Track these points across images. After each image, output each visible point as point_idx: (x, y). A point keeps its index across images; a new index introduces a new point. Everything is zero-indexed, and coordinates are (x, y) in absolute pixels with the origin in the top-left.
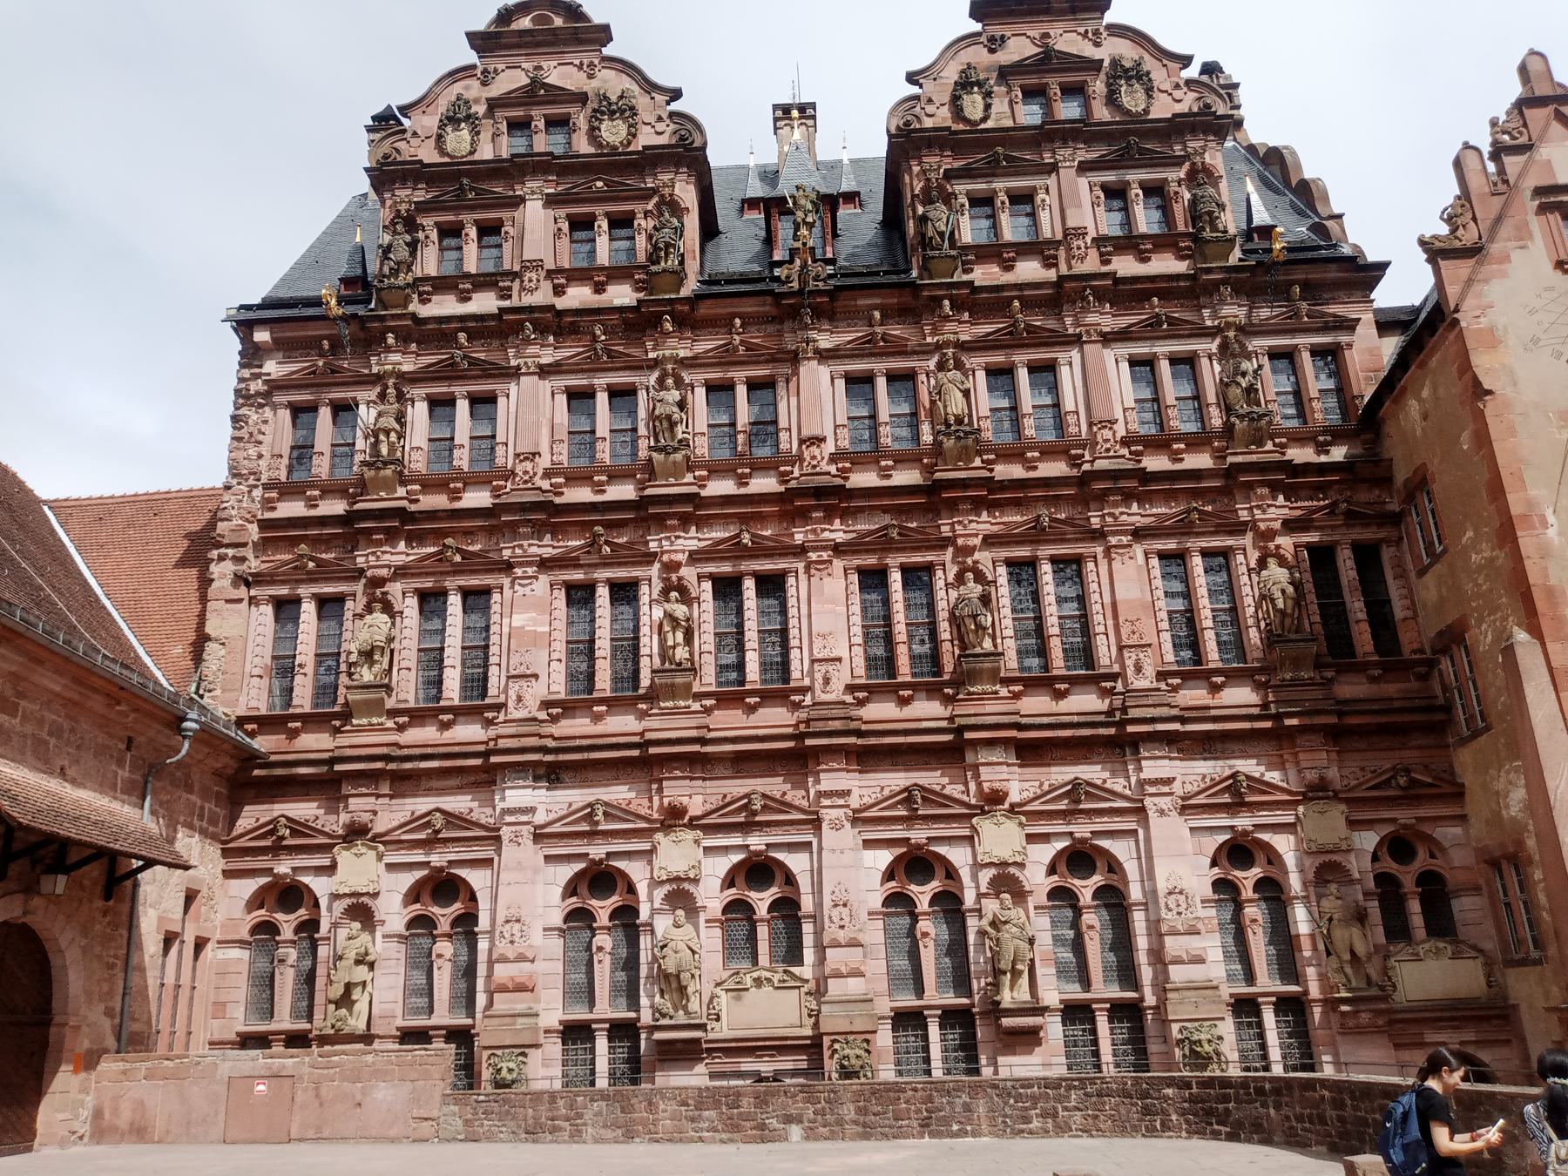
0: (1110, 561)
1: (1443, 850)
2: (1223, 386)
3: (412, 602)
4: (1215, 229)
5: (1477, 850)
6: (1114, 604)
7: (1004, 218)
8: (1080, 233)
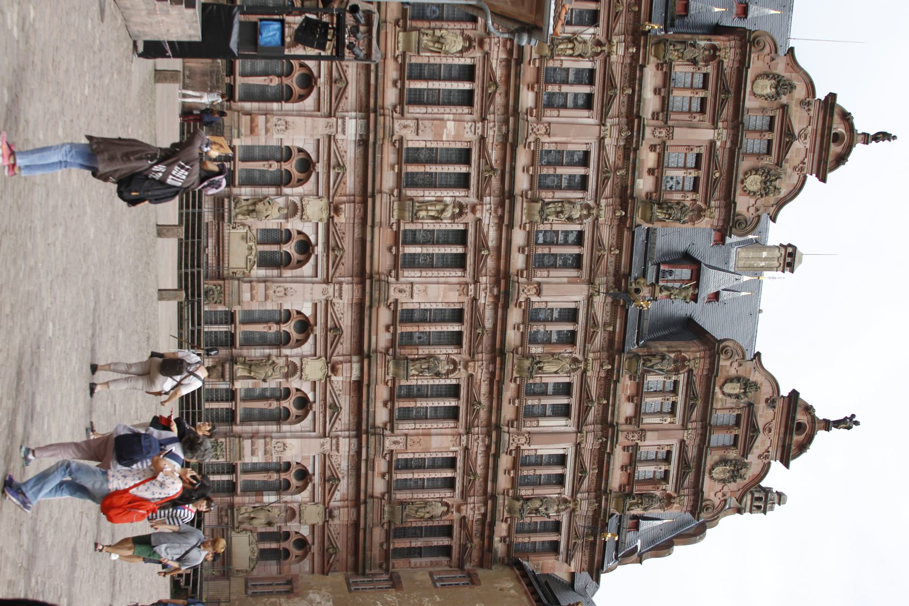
0: (453, 435)
1: (299, 561)
2: (542, 499)
3: (468, 62)
4: (632, 505)
5: (297, 576)
6: (430, 435)
8: (642, 437)
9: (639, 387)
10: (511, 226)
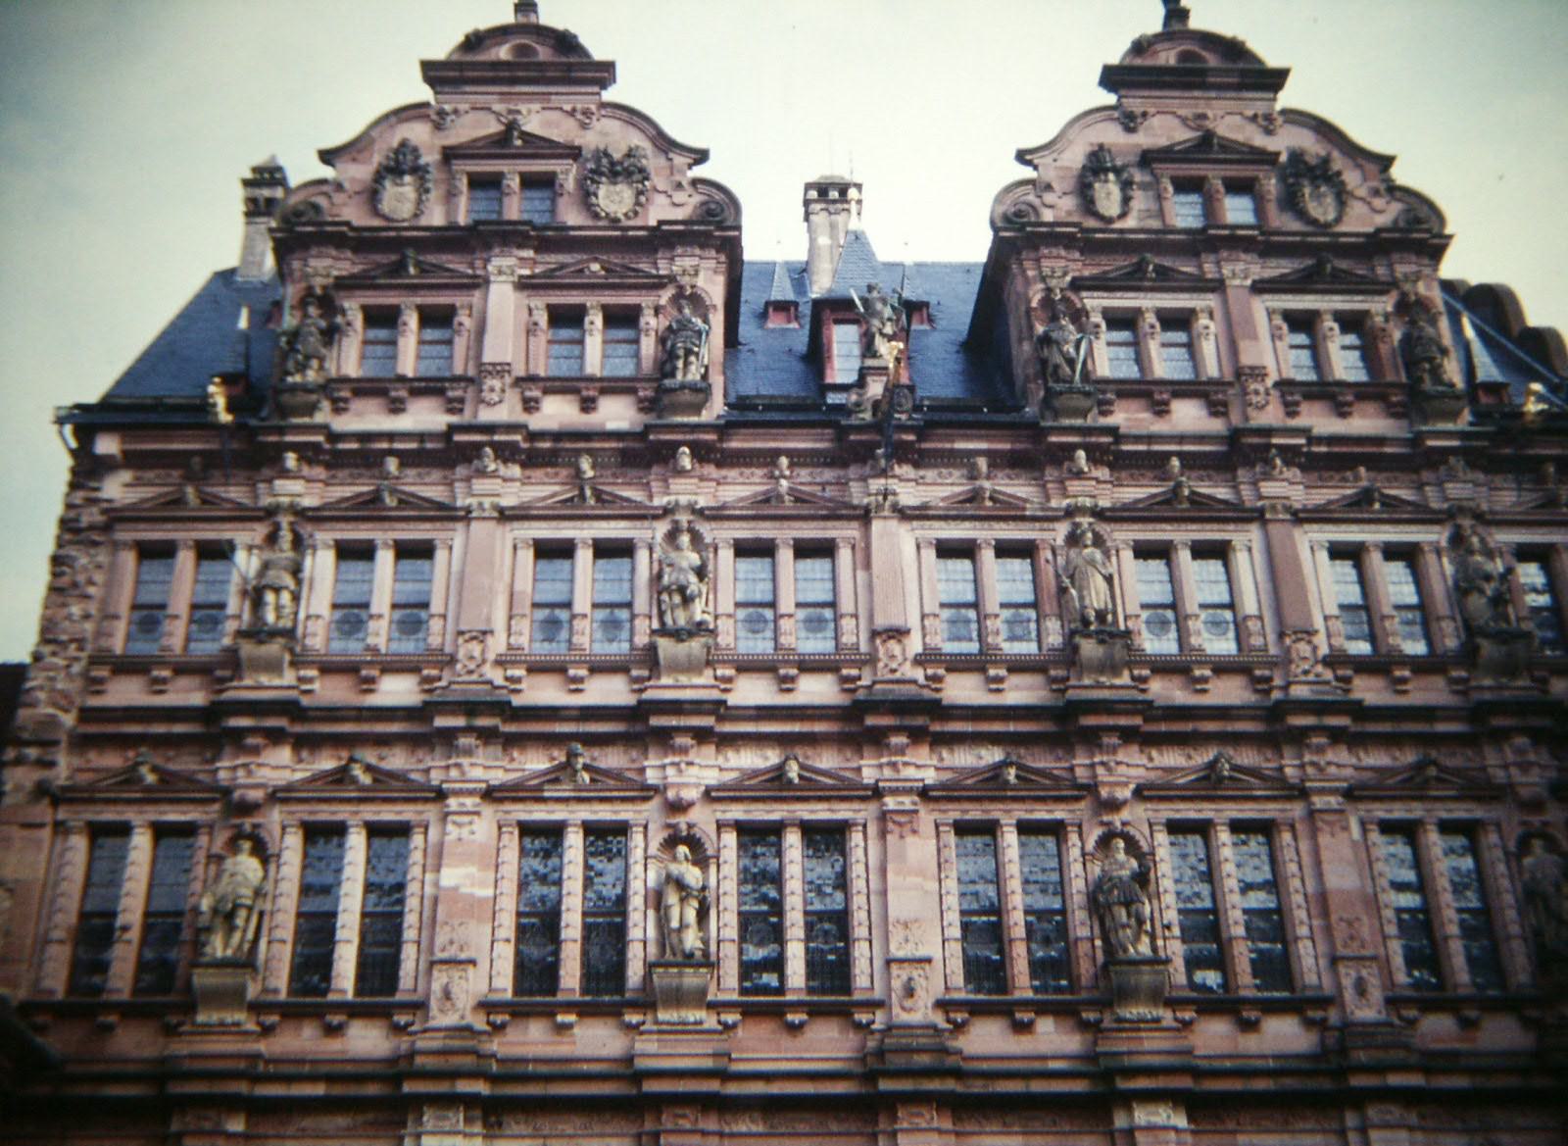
7: (1153, 347)
8: (1258, 373)
9: (1128, 390)
10: (719, 709)
